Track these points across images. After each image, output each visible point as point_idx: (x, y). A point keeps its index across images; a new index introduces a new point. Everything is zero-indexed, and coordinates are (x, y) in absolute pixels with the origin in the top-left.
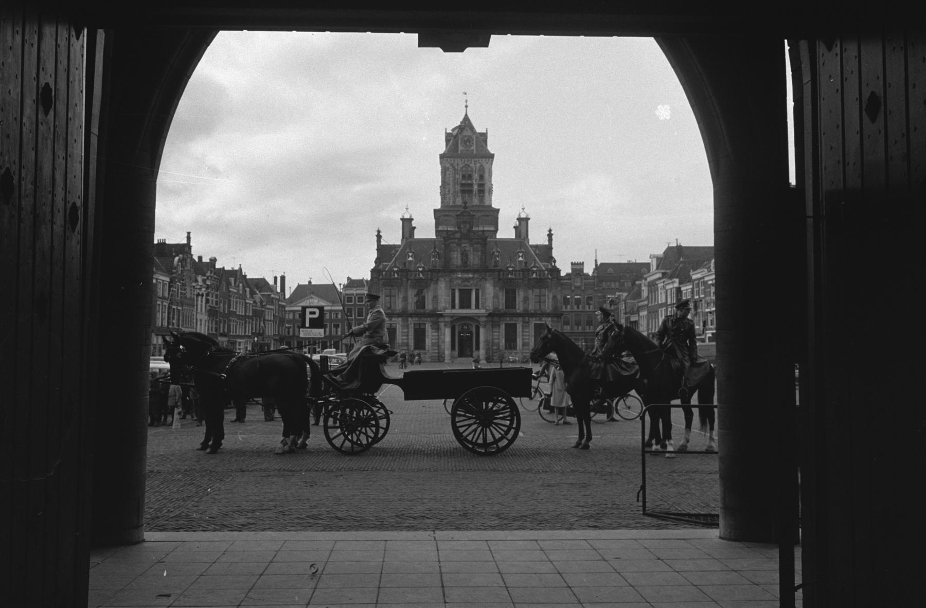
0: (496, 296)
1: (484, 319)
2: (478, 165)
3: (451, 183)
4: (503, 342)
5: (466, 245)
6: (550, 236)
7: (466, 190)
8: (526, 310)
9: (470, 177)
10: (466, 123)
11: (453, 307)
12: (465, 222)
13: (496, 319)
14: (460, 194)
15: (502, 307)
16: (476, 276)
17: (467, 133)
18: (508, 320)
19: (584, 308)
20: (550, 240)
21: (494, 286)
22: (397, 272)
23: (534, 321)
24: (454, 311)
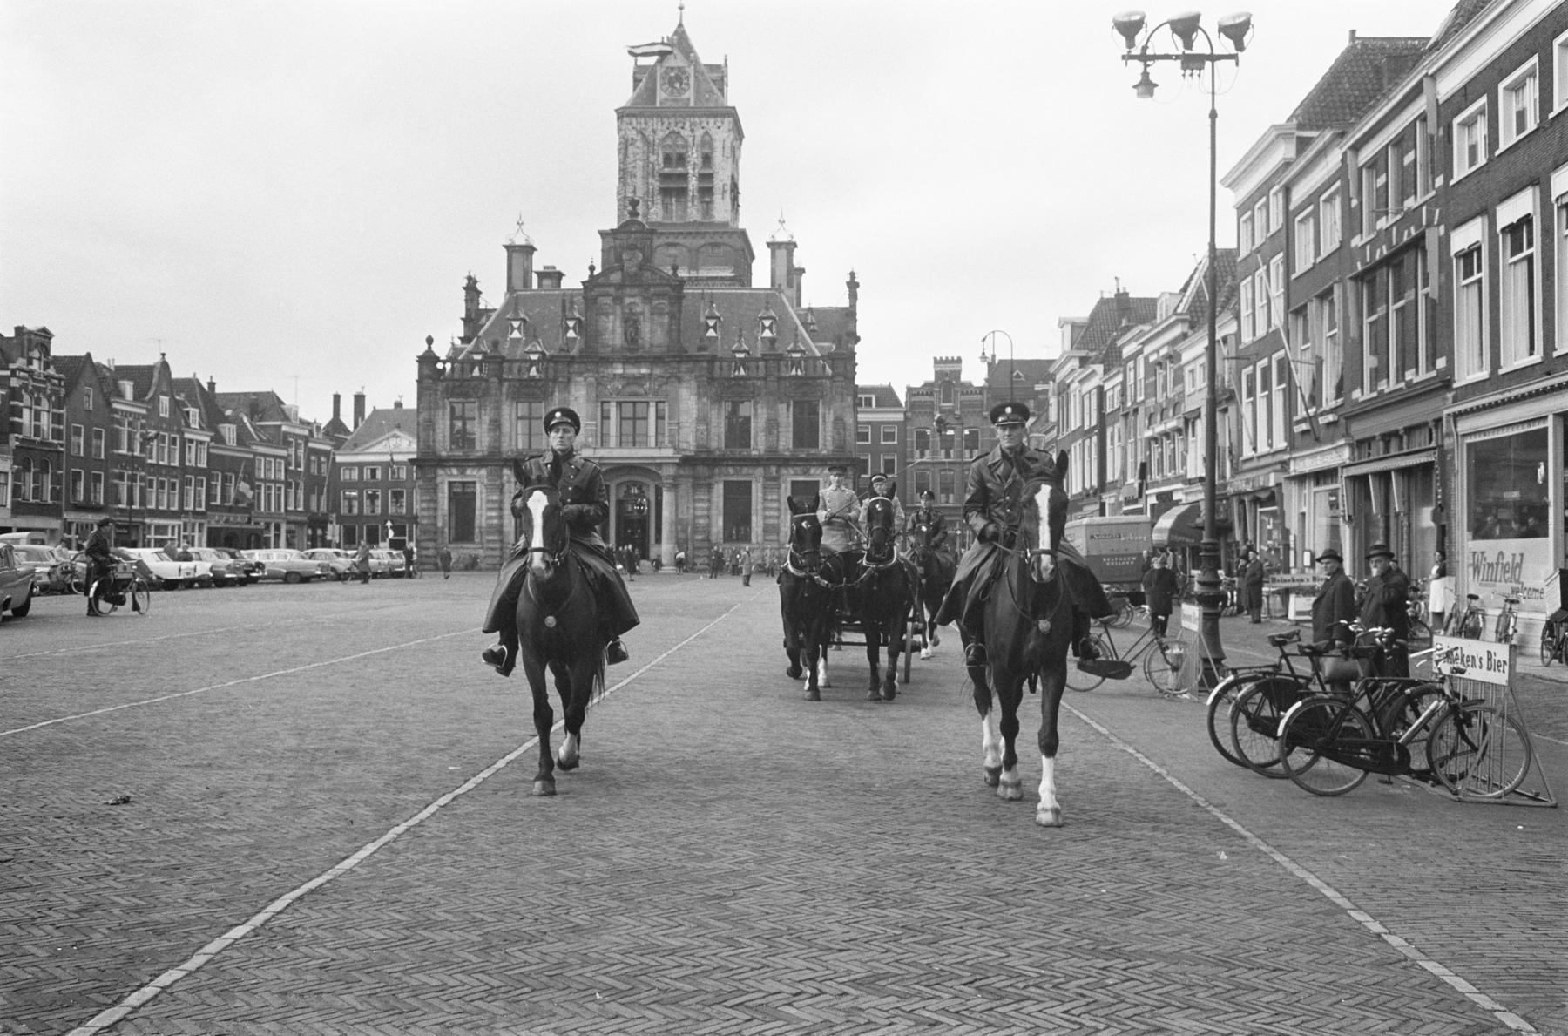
0: (703, 419)
1: (671, 471)
2: (699, 133)
3: (639, 173)
4: (718, 523)
5: (634, 301)
6: (853, 285)
7: (673, 188)
8: (772, 450)
9: (682, 159)
10: (680, 41)
11: (603, 443)
12: (632, 247)
13: (702, 470)
14: (658, 198)
15: (717, 442)
16: (657, 371)
17: (677, 61)
18: (733, 475)
19: (962, 456)
20: (853, 296)
21: (699, 396)
22: (479, 363)
23: (789, 476)
24: (602, 453)
